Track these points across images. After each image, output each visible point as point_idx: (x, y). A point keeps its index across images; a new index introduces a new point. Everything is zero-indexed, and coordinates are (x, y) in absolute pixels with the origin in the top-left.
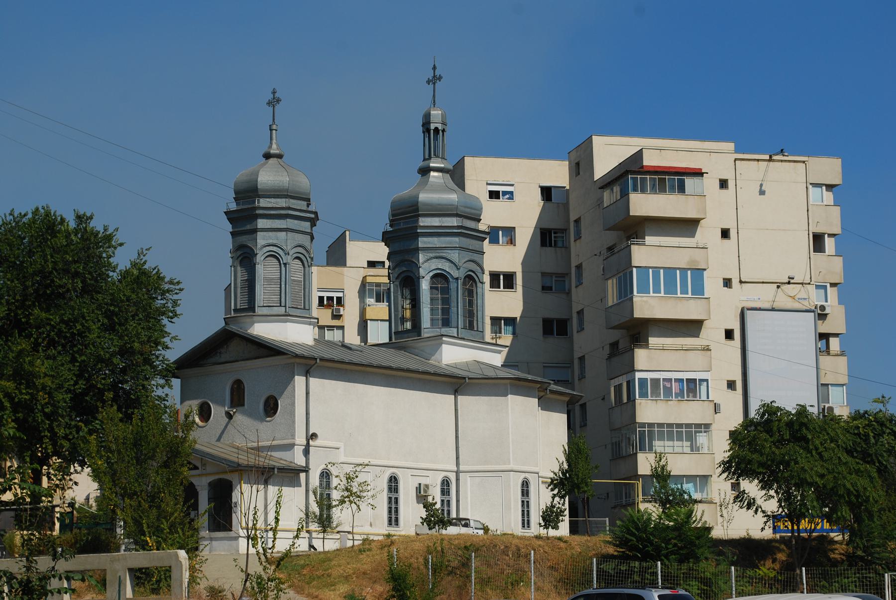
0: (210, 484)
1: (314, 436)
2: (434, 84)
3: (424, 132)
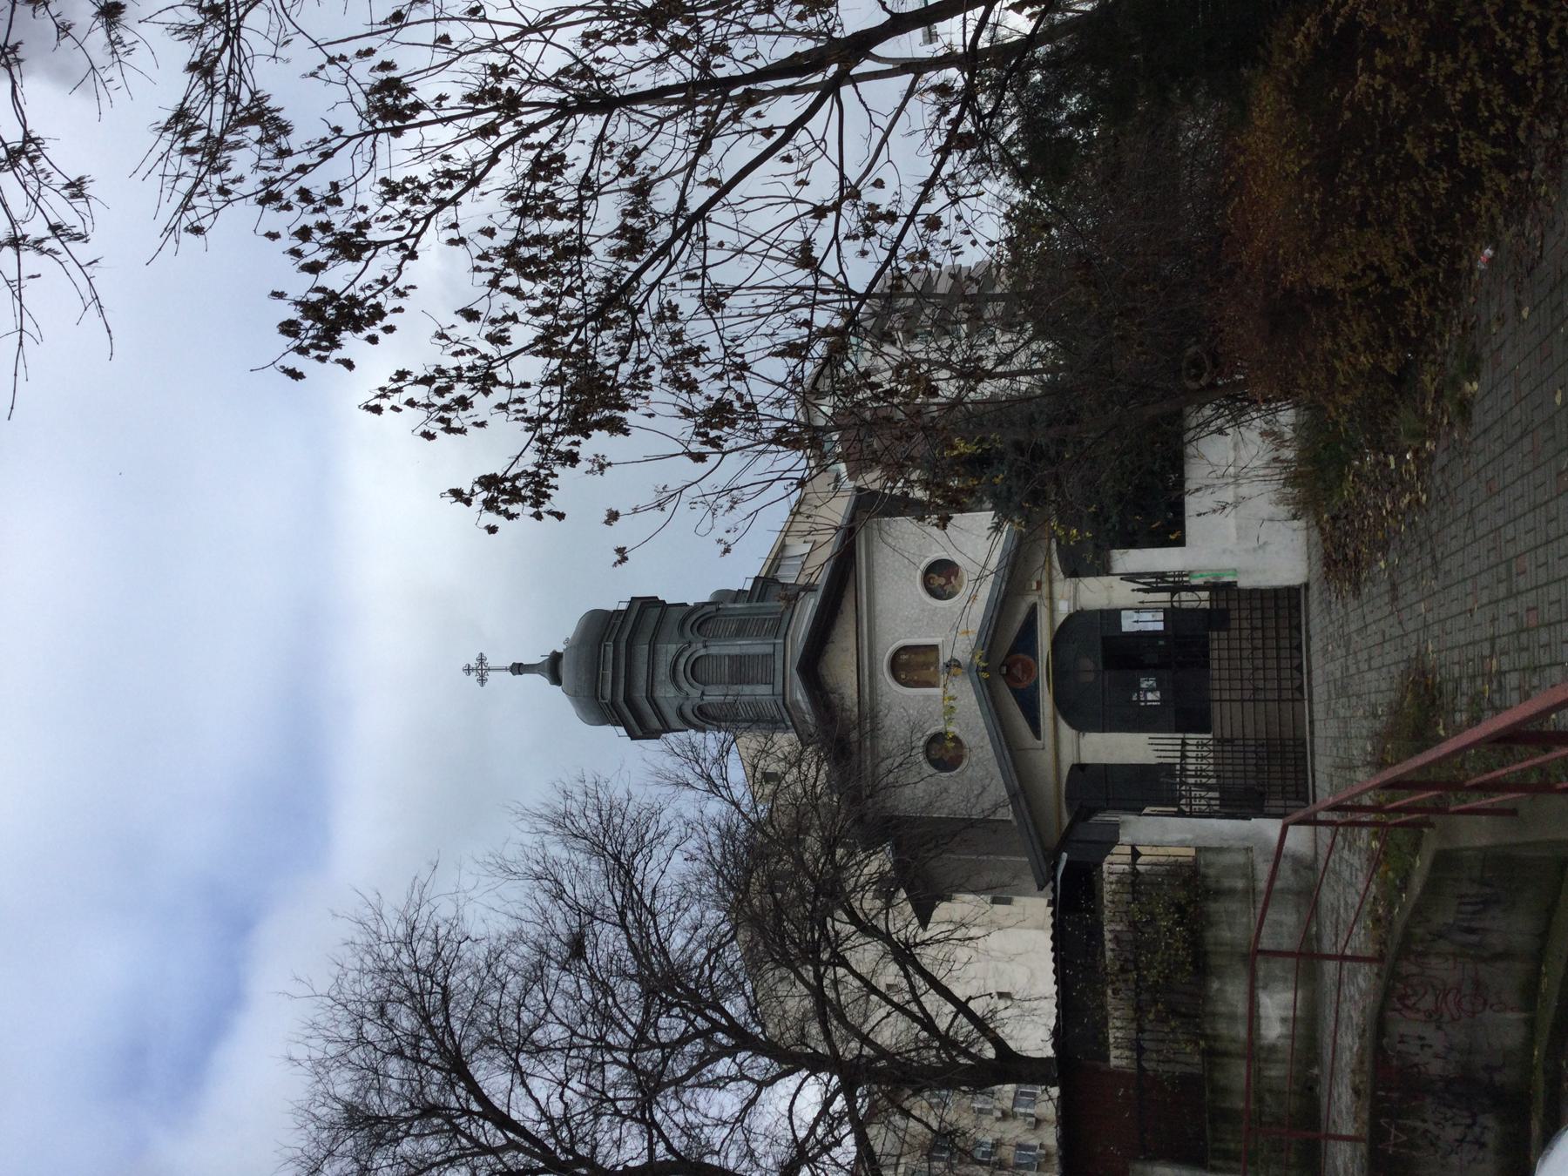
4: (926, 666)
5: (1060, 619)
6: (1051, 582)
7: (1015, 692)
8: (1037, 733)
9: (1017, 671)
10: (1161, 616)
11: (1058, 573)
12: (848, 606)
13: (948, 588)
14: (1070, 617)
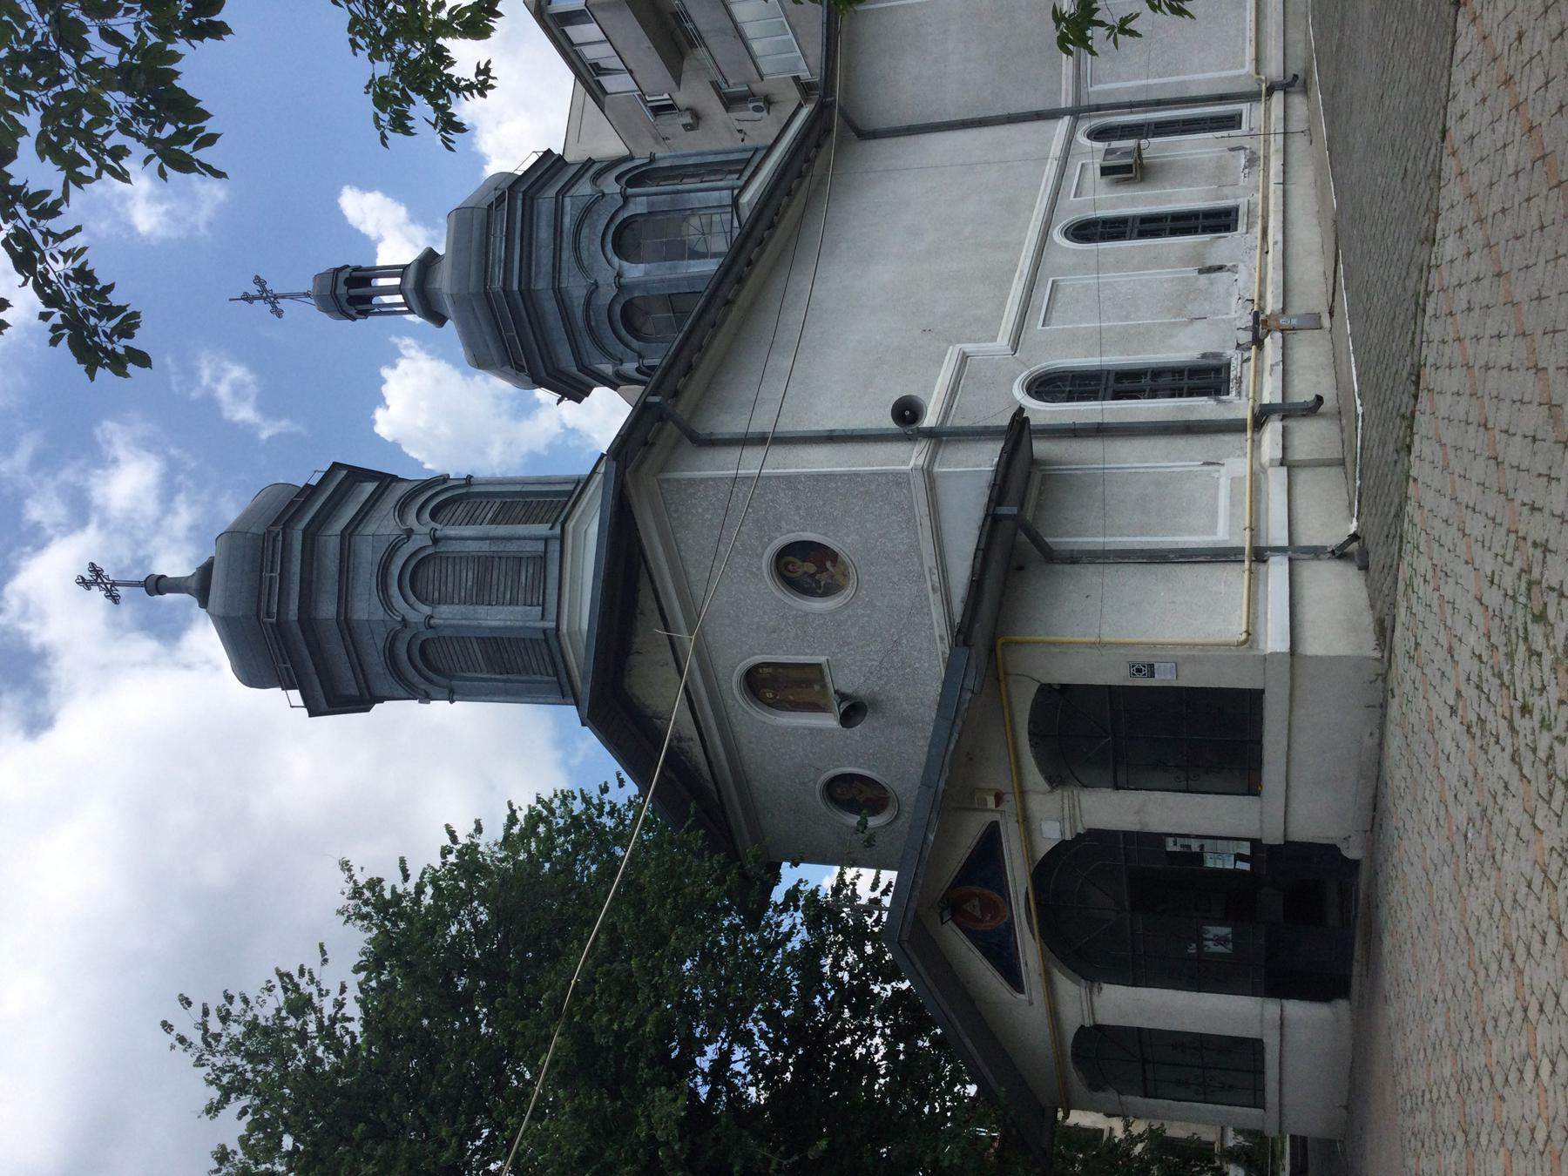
0: (1056, 781)
1: (907, 412)
2: (276, 297)
3: (365, 313)
4: (809, 683)
5: (1044, 847)
6: (1023, 793)
7: (973, 936)
8: (1015, 982)
9: (974, 907)
10: (1245, 849)
11: (1034, 777)
12: (646, 599)
13: (823, 579)
14: (1063, 846)
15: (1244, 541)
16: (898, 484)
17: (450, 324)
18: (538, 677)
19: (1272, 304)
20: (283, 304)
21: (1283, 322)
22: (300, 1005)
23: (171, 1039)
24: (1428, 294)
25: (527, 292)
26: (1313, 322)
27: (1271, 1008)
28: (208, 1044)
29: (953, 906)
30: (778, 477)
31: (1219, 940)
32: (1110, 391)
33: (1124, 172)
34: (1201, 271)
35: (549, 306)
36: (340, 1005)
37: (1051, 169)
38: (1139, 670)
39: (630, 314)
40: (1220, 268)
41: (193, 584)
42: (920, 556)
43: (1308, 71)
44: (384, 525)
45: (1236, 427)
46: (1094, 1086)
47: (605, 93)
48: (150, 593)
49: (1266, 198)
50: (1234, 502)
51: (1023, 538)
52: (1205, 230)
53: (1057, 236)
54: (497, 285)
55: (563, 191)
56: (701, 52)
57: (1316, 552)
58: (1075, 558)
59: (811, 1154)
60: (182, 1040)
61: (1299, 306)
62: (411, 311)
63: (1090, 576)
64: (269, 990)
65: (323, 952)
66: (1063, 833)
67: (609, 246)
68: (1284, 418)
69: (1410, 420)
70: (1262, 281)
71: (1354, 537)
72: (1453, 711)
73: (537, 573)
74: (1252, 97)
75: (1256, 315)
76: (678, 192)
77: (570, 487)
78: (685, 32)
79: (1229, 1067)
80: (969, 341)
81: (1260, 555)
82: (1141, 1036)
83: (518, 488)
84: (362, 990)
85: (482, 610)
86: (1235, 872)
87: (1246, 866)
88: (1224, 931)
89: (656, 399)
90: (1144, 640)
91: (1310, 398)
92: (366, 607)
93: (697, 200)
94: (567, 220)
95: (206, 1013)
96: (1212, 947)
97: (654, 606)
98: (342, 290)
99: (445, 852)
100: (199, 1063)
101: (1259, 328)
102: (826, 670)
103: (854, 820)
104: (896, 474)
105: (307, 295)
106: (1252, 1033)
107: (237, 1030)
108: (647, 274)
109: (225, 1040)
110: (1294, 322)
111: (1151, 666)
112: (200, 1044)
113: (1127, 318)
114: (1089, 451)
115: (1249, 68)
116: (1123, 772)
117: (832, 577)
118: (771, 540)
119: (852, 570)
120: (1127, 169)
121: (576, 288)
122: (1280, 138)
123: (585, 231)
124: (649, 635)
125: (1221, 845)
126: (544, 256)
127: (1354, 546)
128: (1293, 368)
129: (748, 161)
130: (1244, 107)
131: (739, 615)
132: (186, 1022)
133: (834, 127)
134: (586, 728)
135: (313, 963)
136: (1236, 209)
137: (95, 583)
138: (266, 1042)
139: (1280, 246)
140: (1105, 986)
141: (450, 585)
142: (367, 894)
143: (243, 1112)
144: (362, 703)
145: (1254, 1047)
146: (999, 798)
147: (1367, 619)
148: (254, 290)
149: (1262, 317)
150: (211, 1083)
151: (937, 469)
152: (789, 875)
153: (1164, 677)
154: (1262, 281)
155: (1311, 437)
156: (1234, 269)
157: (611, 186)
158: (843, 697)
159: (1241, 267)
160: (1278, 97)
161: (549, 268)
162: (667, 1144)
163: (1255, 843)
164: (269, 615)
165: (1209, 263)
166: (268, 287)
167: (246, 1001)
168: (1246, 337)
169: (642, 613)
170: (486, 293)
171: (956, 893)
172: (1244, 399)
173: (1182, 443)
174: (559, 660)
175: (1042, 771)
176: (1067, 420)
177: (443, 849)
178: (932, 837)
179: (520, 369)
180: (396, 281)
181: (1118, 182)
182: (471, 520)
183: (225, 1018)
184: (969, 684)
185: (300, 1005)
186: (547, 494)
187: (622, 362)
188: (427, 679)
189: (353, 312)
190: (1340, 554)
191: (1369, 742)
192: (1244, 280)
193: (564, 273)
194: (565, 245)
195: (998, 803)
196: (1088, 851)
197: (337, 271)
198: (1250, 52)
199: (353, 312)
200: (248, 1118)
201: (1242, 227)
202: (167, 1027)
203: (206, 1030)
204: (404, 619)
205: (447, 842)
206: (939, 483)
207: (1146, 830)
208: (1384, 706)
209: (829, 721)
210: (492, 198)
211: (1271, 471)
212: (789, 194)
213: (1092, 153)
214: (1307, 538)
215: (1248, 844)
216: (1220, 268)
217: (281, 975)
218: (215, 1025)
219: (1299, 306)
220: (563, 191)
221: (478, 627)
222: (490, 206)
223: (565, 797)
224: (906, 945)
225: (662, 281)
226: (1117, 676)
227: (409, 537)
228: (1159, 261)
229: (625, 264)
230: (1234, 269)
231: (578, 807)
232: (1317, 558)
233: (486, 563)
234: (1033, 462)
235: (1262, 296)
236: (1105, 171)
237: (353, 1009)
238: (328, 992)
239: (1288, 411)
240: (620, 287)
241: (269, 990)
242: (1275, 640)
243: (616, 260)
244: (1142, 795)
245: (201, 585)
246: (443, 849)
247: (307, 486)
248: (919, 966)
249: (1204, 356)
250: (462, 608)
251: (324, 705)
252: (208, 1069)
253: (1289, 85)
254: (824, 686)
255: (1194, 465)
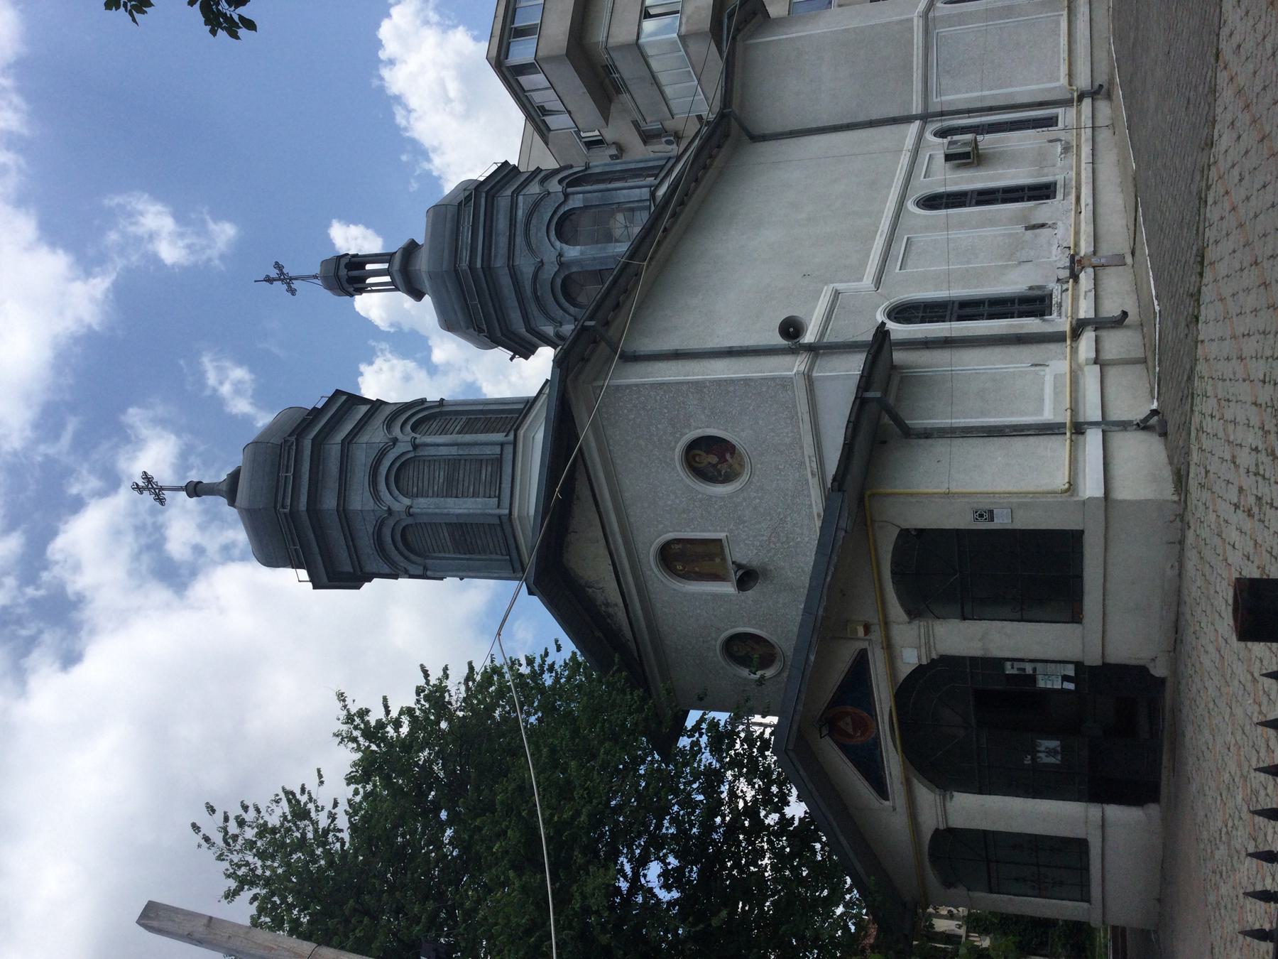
0: (914, 613)
1: (791, 329)
2: (291, 279)
3: (361, 291)
6: (886, 624)
7: (844, 748)
8: (882, 791)
9: (847, 724)
10: (1070, 671)
12: (582, 490)
13: (724, 468)
14: (920, 671)
15: (1066, 418)
16: (784, 386)
17: (427, 299)
18: (494, 557)
19: (1085, 248)
20: (296, 284)
21: (1094, 261)
22: (300, 813)
23: (198, 838)
24: (1208, 188)
25: (488, 268)
26: (1119, 261)
27: (1094, 811)
28: (228, 844)
29: (830, 723)
30: (688, 383)
31: (1050, 752)
32: (955, 315)
33: (963, 159)
34: (1027, 228)
35: (505, 281)
36: (332, 817)
37: (905, 160)
38: (981, 516)
39: (568, 285)
40: (1043, 226)
41: (224, 488)
42: (802, 448)
43: (1111, 81)
44: (376, 435)
45: (1058, 338)
46: (948, 884)
47: (549, 130)
48: (190, 496)
49: (1078, 174)
50: (1057, 393)
51: (886, 419)
52: (1029, 199)
53: (910, 206)
54: (464, 265)
55: (517, 192)
56: (625, 97)
57: (1124, 425)
58: (927, 434)
59: (715, 922)
60: (207, 839)
61: (1106, 249)
62: (397, 289)
63: (940, 447)
64: (277, 802)
65: (320, 776)
66: (919, 658)
67: (553, 233)
68: (1096, 329)
69: (1196, 296)
70: (1077, 233)
71: (1154, 412)
72: (1237, 506)
73: (494, 472)
74: (1066, 103)
75: (1072, 257)
76: (609, 190)
77: (521, 406)
78: (614, 82)
79: (1062, 861)
80: (841, 281)
81: (1079, 429)
82: (986, 837)
83: (481, 407)
84: (350, 805)
85: (450, 501)
86: (1063, 691)
87: (1071, 686)
88: (1054, 744)
89: (592, 323)
90: (985, 490)
91: (1117, 313)
92: (360, 500)
93: (623, 196)
94: (520, 213)
95: (226, 819)
96: (1044, 759)
97: (589, 493)
98: (343, 272)
99: (419, 691)
100: (220, 858)
101: (1075, 267)
102: (725, 544)
103: (745, 672)
104: (783, 378)
105: (315, 277)
106: (1078, 833)
107: (250, 833)
108: (582, 253)
109: (240, 841)
110: (1103, 261)
111: (991, 512)
112: (222, 844)
113: (968, 262)
114: (939, 359)
115: (1063, 81)
116: (972, 602)
117: (731, 466)
118: (683, 435)
119: (746, 459)
120: (966, 155)
121: (526, 266)
122: (1089, 131)
123: (534, 221)
124: (584, 516)
125: (1051, 667)
126: (503, 241)
127: (1156, 418)
128: (1102, 293)
129: (662, 167)
130: (1060, 111)
131: (659, 500)
132: (211, 826)
133: (730, 136)
134: (535, 599)
135: (312, 785)
136: (1055, 184)
137: (147, 488)
138: (274, 842)
139: (1091, 207)
140: (955, 794)
141: (426, 483)
142: (357, 721)
143: (255, 898)
144: (354, 580)
145: (1079, 847)
146: (867, 629)
147: (1167, 473)
148: (274, 273)
149: (1077, 258)
150: (229, 876)
151: (815, 374)
152: (693, 717)
153: (1002, 521)
154: (1077, 233)
155: (1118, 343)
156: (1054, 226)
157: (554, 186)
158: (739, 566)
159: (1060, 224)
160: (1087, 103)
161: (506, 251)
162: (598, 913)
163: (1079, 665)
164: (283, 507)
165: (1034, 222)
166: (285, 271)
167: (258, 811)
168: (1066, 273)
169: (578, 499)
170: (456, 271)
171: (830, 721)
172: (1064, 318)
173: (1013, 350)
174: (511, 541)
175: (902, 605)
176: (920, 336)
177: (418, 688)
178: (812, 658)
179: (480, 331)
180: (385, 266)
181: (959, 167)
182: (443, 431)
183: (241, 823)
184: (843, 524)
185: (300, 813)
186: (503, 411)
187: (561, 325)
188: (406, 558)
189: (351, 290)
190: (1143, 426)
191: (1170, 573)
192: (1064, 232)
193: (517, 253)
194: (518, 233)
195: (866, 634)
196: (942, 672)
197: (340, 257)
198: (1064, 69)
199: (351, 290)
200: (256, 904)
201: (1059, 195)
202: (195, 827)
203: (226, 833)
204: (389, 509)
205: (422, 682)
206: (816, 384)
207: (989, 655)
208: (1182, 542)
209: (728, 588)
210: (462, 197)
211: (1087, 369)
212: (696, 180)
213: (937, 147)
214: (1116, 415)
215: (1071, 667)
216: (1043, 226)
217: (287, 793)
218: (233, 828)
219: (1106, 249)
220: (517, 192)
221: (448, 514)
222: (460, 204)
223: (513, 663)
224: (791, 754)
225: (595, 259)
226: (962, 520)
227: (394, 444)
228: (991, 222)
229: (565, 247)
230: (1054, 226)
231: (525, 670)
232: (1125, 429)
233: (453, 464)
234: (893, 367)
235: (1077, 244)
236: (948, 158)
237: (343, 822)
238: (323, 808)
239: (1100, 324)
240: (561, 264)
241: (277, 802)
242: (1092, 487)
243: (558, 244)
244: (985, 624)
245: (230, 490)
246: (418, 688)
247: (315, 408)
248: (802, 772)
249: (1031, 288)
250: (435, 500)
251: (325, 580)
252: (226, 865)
253: (1095, 93)
254: (724, 559)
255: (1024, 366)
